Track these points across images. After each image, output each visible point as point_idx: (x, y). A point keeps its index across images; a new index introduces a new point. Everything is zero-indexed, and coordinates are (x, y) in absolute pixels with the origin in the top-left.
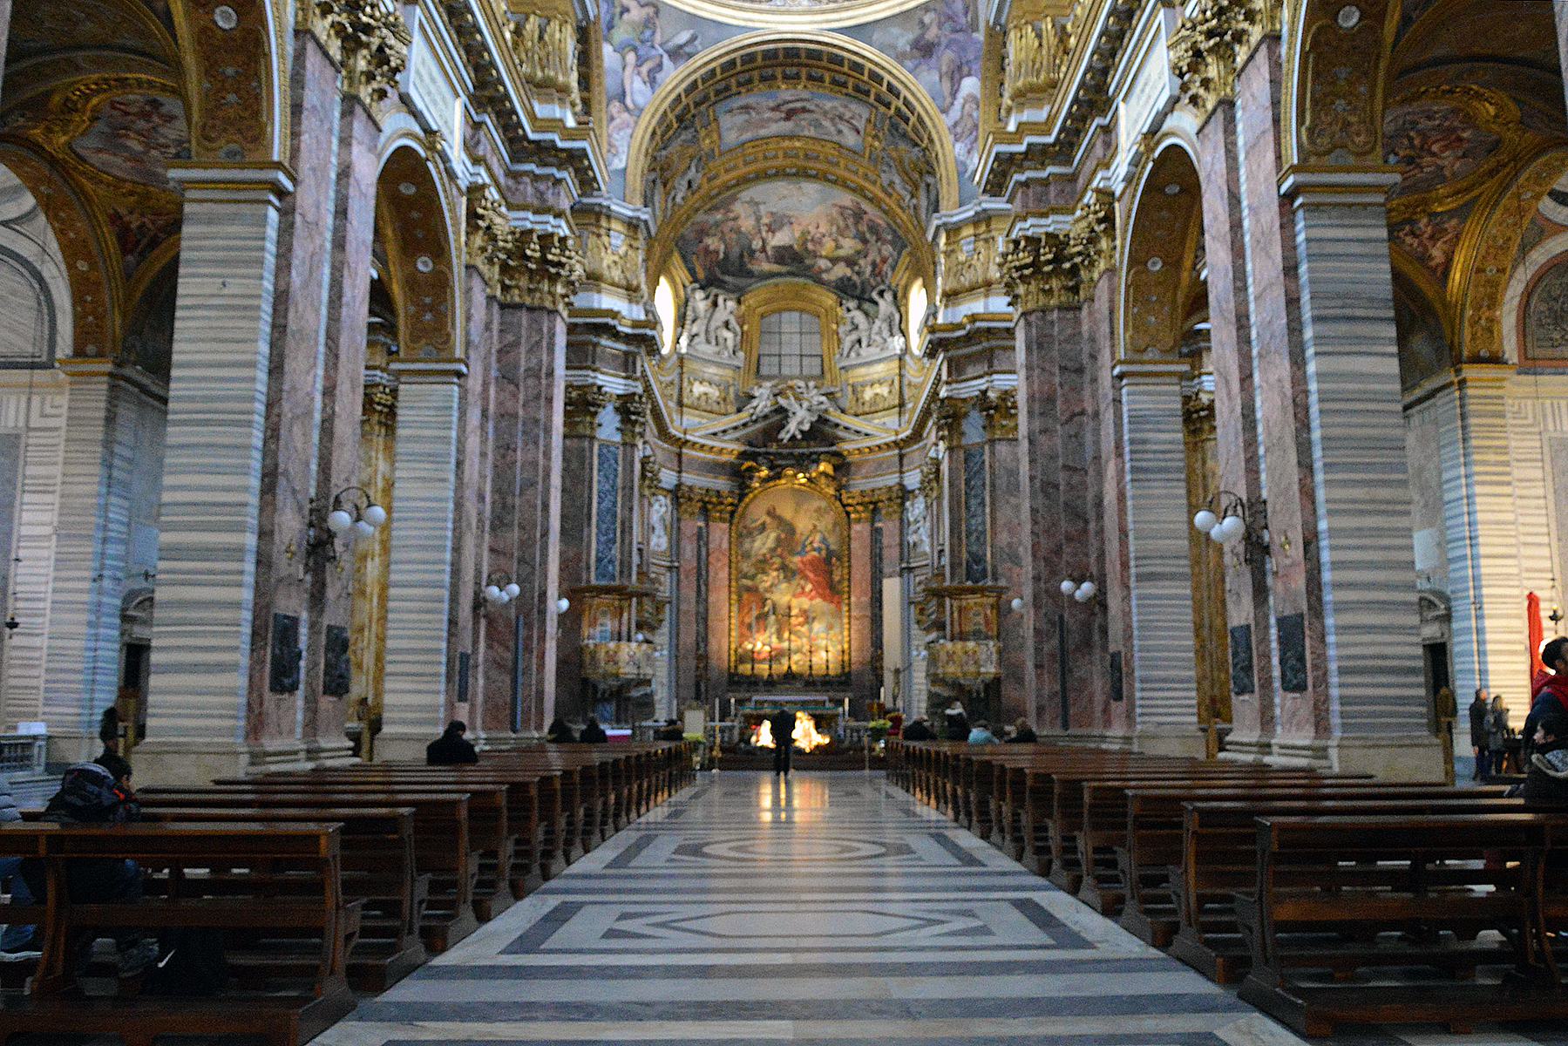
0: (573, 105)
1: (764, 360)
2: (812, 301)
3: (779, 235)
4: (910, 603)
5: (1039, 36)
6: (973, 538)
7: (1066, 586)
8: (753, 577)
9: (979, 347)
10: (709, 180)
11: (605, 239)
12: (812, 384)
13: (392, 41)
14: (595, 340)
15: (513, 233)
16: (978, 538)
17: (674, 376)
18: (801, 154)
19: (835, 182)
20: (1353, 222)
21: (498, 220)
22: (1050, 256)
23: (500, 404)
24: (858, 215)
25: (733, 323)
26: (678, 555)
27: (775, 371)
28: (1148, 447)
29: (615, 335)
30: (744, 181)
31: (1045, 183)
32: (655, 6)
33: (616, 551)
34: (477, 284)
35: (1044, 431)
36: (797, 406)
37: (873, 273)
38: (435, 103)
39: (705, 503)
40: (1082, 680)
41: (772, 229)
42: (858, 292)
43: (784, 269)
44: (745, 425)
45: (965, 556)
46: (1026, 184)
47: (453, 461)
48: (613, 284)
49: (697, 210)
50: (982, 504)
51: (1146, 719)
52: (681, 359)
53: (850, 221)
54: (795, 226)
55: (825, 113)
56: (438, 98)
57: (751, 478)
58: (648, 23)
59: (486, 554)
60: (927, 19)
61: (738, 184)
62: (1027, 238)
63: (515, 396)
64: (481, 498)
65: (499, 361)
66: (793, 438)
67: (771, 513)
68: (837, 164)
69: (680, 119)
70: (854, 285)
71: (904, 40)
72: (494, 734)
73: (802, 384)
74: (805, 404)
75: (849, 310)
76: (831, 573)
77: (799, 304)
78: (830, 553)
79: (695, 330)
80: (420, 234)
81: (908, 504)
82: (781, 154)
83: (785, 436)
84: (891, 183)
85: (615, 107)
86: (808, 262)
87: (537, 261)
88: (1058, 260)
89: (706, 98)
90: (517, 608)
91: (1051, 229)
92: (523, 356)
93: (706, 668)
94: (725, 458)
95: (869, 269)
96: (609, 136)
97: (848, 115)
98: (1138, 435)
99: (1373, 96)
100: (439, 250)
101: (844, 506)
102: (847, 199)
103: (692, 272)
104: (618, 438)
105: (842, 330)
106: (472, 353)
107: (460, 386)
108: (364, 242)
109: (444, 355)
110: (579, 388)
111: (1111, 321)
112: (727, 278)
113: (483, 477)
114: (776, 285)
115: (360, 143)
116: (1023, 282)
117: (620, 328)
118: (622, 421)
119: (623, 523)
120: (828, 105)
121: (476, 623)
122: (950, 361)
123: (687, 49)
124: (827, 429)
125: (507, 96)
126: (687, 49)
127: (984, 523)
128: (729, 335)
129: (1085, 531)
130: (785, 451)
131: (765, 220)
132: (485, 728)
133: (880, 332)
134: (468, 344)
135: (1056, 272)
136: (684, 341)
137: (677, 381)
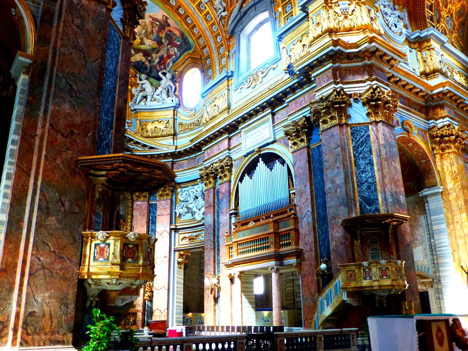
6: (365, 187)
9: (360, 64)
16: (369, 187)
37: (159, 63)
42: (148, 71)
45: (358, 199)
50: (371, 163)
70: (146, 68)
75: (141, 80)
95: (157, 60)
122: (335, 70)
127: (373, 177)
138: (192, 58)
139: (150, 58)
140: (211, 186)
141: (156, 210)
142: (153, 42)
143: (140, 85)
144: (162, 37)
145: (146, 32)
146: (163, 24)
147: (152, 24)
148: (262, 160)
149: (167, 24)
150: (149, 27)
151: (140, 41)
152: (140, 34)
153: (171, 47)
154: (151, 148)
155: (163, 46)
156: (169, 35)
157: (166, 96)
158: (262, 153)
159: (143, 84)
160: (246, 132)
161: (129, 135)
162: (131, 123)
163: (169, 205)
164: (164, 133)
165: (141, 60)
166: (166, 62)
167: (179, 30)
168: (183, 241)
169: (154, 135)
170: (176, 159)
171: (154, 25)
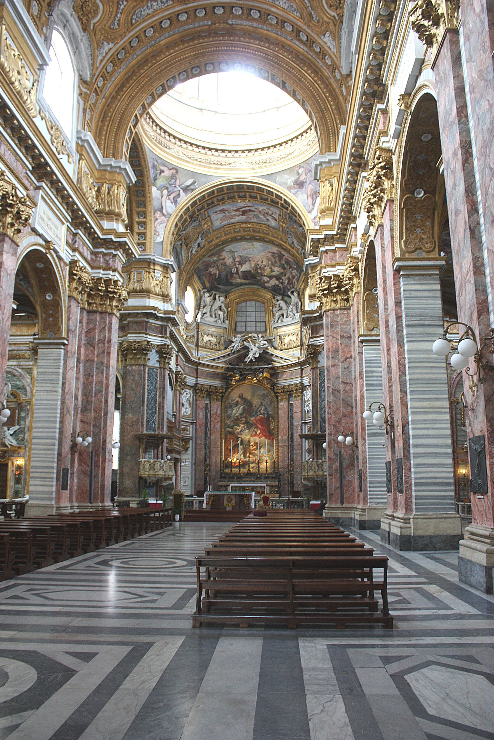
0: (123, 221)
1: (239, 324)
2: (261, 296)
3: (244, 266)
5: (332, 185)
7: (340, 438)
8: (232, 427)
10: (209, 243)
11: (152, 274)
12: (260, 335)
13: (23, 208)
14: (146, 320)
15: (93, 279)
17: (195, 333)
18: (251, 229)
19: (268, 242)
20: (425, 282)
21: (84, 275)
22: (335, 285)
23: (86, 356)
24: (281, 256)
25: (223, 307)
26: (196, 417)
27: (243, 329)
28: (374, 374)
29: (157, 318)
30: (226, 242)
31: (334, 251)
32: (176, 169)
33: (156, 417)
34: (73, 304)
35: (334, 366)
36: (253, 346)
38: (51, 229)
40: (350, 482)
41: (241, 264)
43: (247, 282)
44: (229, 355)
45: (319, 419)
46: (326, 252)
47: (61, 383)
48: (156, 294)
49: (204, 256)
51: (371, 500)
52: (198, 325)
53: (277, 259)
54: (252, 262)
55: (260, 212)
56: (53, 227)
57: (231, 380)
58: (173, 177)
59: (78, 423)
60: (300, 171)
61: (223, 244)
62: (325, 277)
63: (93, 352)
64: (76, 398)
65: (86, 336)
66: (251, 360)
67: (241, 396)
68: (268, 234)
69: (191, 217)
70: (280, 289)
71: (290, 180)
72: (82, 504)
73: (256, 335)
74: (257, 345)
78: (269, 416)
79: (204, 311)
80: (47, 284)
82: (241, 229)
83: (247, 360)
84: (293, 242)
85: (158, 214)
86: (258, 278)
87: (104, 291)
88: (339, 287)
89: (203, 208)
90: (93, 447)
91: (336, 273)
92: (97, 334)
93: (210, 470)
94: (219, 371)
95: (287, 282)
96: (155, 227)
97: (270, 213)
98: (370, 369)
99: (433, 227)
100: (55, 290)
101: (275, 393)
102: (275, 249)
103: (203, 284)
104: (157, 365)
105: (274, 310)
106: (70, 335)
107: (64, 349)
108: (9, 294)
109: (57, 336)
110: (138, 342)
111: (358, 316)
112: (220, 286)
113: (77, 389)
114: (244, 289)
115: (8, 253)
116: (325, 297)
117: (158, 315)
118: (160, 357)
119: (159, 404)
120: (261, 208)
121: (73, 454)
123: (192, 187)
125: (88, 221)
126: (192, 187)
128: (221, 313)
129: (352, 412)
132: (78, 501)
133: (292, 311)
134: (68, 331)
135: (339, 293)
136: (199, 316)
147: (273, 256)
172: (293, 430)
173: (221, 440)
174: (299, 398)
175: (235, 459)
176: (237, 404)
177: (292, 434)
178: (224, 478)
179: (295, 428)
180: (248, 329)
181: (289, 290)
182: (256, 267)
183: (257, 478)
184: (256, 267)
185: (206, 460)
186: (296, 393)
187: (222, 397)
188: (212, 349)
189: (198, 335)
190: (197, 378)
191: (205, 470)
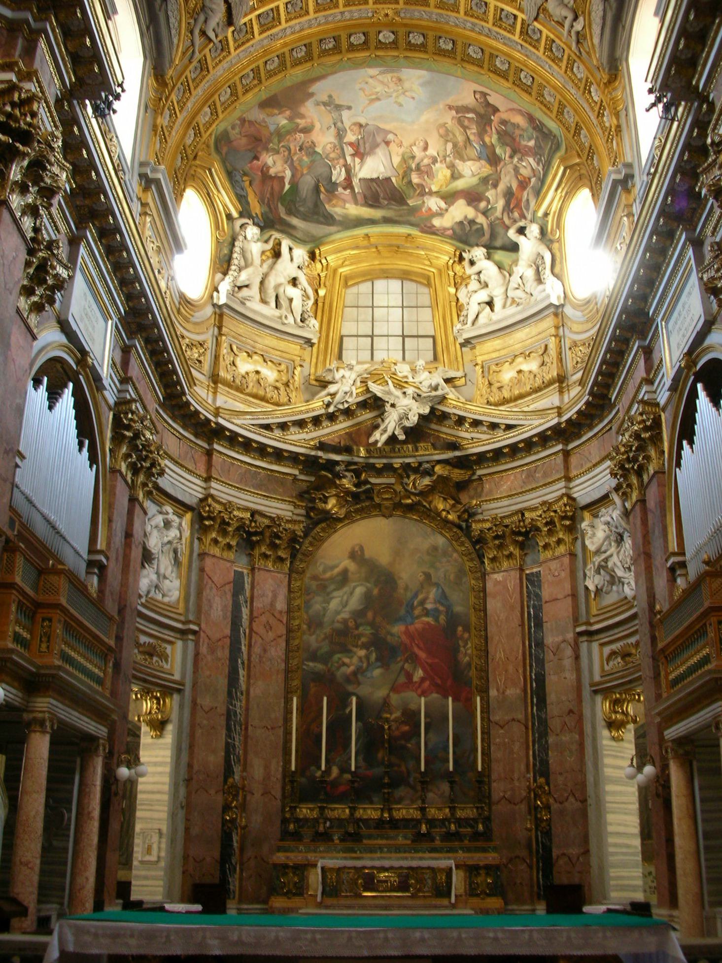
1: (348, 343)
4: (596, 692)
17: (208, 337)
36: (398, 393)
37: (507, 208)
39: (250, 534)
41: (360, 154)
43: (377, 214)
44: (317, 421)
53: (473, 130)
54: (393, 146)
61: (309, 57)
66: (393, 439)
67: (356, 555)
70: (480, 231)
74: (410, 391)
76: (456, 650)
77: (402, 264)
79: (244, 277)
81: (584, 525)
83: (379, 437)
86: (411, 202)
93: (243, 807)
95: (501, 204)
103: (241, 198)
105: (462, 294)
112: (295, 221)
114: (367, 236)
124: (447, 431)
130: (379, 462)
131: (351, 137)
136: (225, 286)
137: (210, 344)
138: (571, 167)
139: (483, 205)
140: (635, 496)
141: (540, 587)
142: (478, 164)
143: (473, 277)
144: (493, 145)
145: (455, 146)
146: (482, 111)
147: (460, 122)
148: (706, 388)
149: (490, 110)
150: (457, 134)
151: (448, 173)
152: (445, 157)
153: (521, 160)
154: (509, 427)
155: (502, 163)
156: (506, 133)
157: (535, 284)
158: (698, 367)
159: (480, 272)
160: (667, 318)
161: (455, 407)
162: (465, 376)
163: (568, 571)
164: (538, 382)
165: (466, 217)
166: (521, 200)
167: (520, 112)
168: (611, 663)
169: (517, 392)
170: (573, 441)
171: (466, 123)
172: (541, 663)
173: (288, 701)
174: (562, 549)
175: (335, 771)
176: (344, 578)
177: (541, 680)
178: (296, 836)
179: (549, 656)
180: (379, 356)
181: (507, 228)
182: (408, 166)
183: (419, 837)
184: (408, 166)
185: (228, 771)
186: (550, 533)
187: (293, 556)
188: (263, 399)
189: (218, 344)
190: (207, 479)
191: (227, 808)
